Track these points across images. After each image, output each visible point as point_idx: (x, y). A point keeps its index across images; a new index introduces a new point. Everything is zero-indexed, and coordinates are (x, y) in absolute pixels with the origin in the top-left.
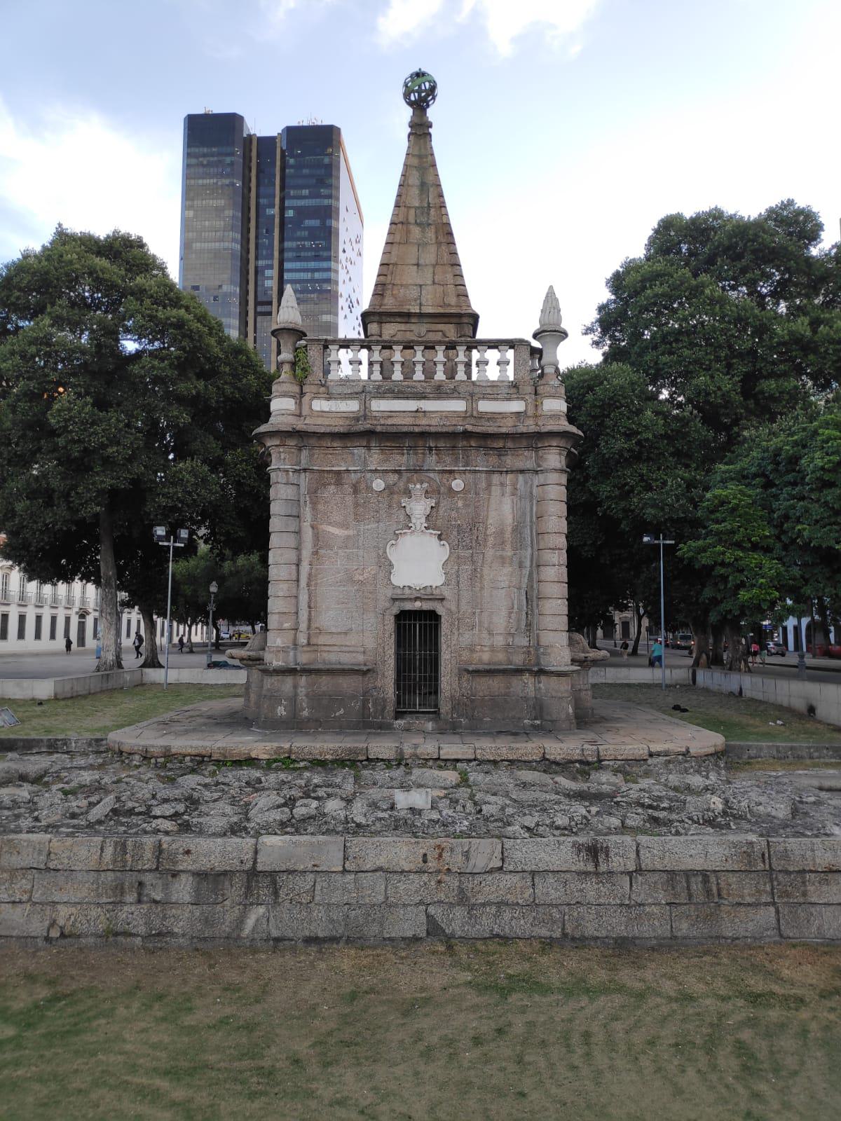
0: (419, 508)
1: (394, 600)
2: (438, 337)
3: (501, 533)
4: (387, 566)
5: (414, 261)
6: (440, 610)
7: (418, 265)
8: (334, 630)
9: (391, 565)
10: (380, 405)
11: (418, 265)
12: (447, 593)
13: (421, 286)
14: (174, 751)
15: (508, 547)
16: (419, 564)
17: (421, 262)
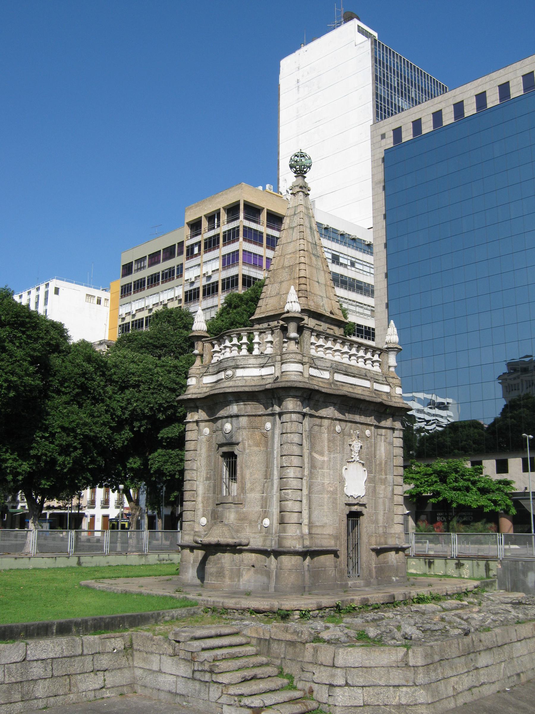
0: (357, 445)
1: (346, 504)
2: (331, 332)
3: (380, 464)
4: (342, 481)
5: (316, 280)
6: (364, 510)
7: (318, 282)
10: (339, 377)
11: (318, 282)
12: (364, 501)
13: (322, 297)
14: (323, 605)
15: (383, 473)
16: (355, 483)
17: (320, 281)
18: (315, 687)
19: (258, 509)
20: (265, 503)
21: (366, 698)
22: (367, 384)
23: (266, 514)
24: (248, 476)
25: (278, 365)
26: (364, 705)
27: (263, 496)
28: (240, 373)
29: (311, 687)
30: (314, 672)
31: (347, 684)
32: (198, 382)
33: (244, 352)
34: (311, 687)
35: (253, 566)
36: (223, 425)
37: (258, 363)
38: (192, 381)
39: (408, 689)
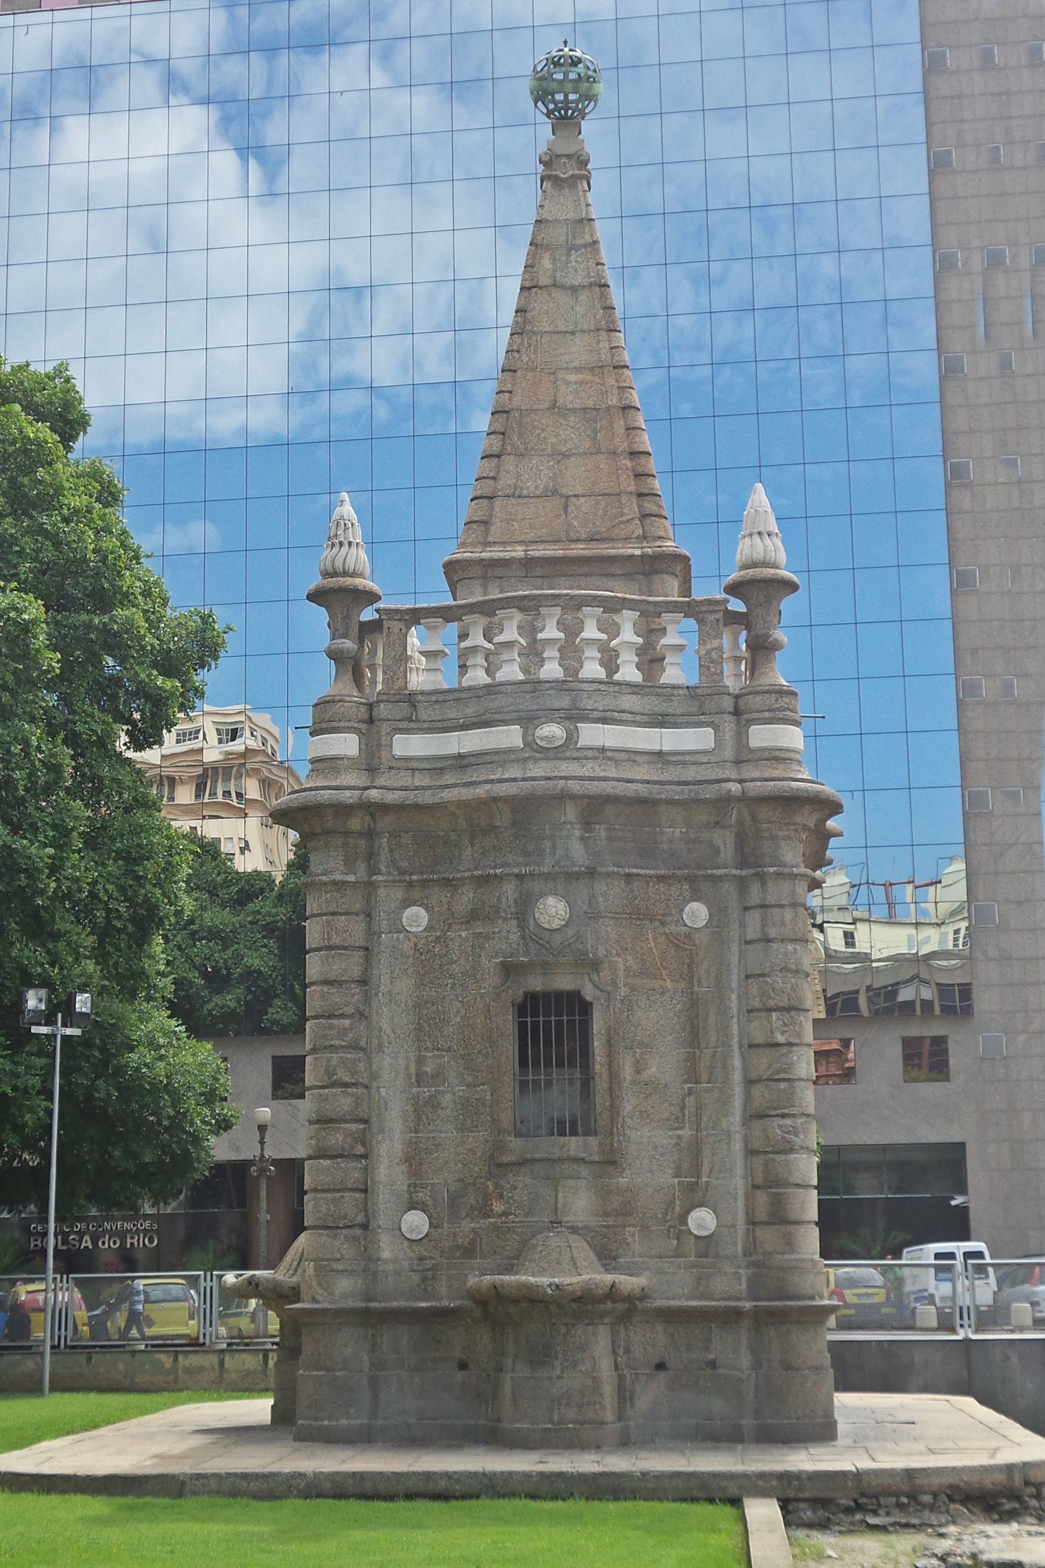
19: (667, 1179)
20: (691, 1159)
23: (694, 1195)
24: (627, 1073)
25: (729, 724)
27: (679, 1137)
28: (592, 735)
37: (647, 709)
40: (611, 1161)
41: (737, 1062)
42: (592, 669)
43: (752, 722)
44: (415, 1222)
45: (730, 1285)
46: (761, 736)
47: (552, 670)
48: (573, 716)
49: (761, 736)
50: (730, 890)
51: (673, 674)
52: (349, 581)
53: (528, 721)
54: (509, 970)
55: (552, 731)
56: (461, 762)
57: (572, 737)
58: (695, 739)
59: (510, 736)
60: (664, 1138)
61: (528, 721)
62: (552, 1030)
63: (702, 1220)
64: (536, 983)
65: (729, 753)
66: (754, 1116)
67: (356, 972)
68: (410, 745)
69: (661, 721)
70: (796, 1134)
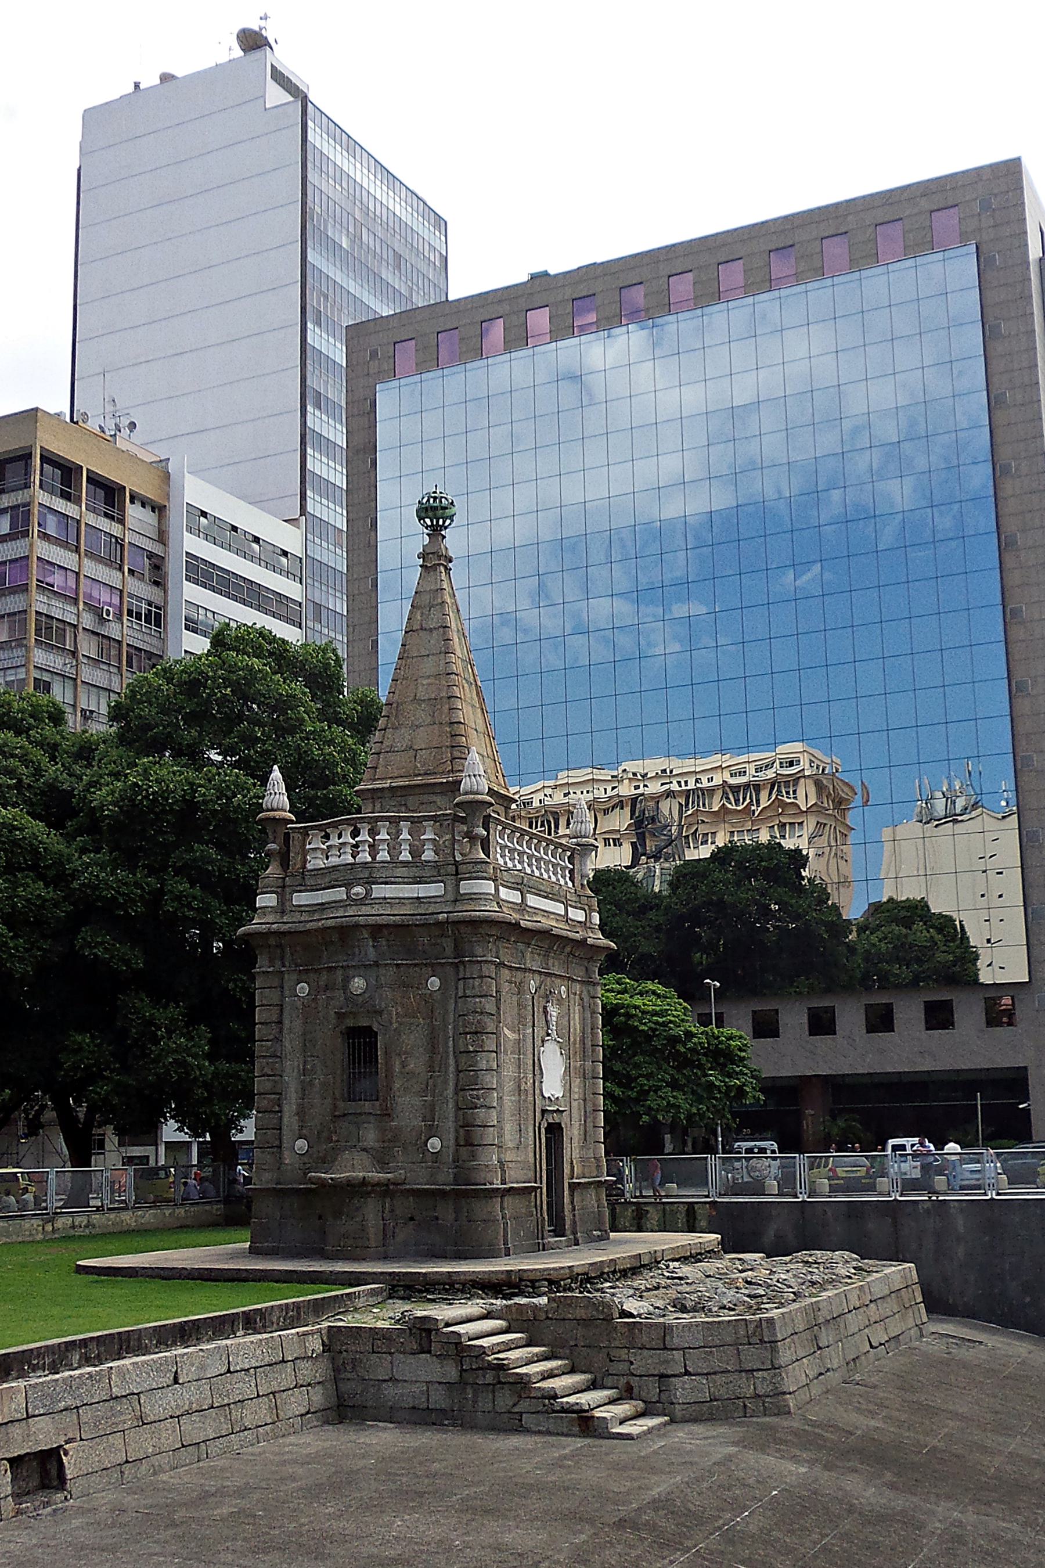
1: (544, 1112)
8: (510, 1145)
9: (542, 1073)
10: (532, 900)
18: (634, 1381)
19: (418, 1123)
20: (430, 1114)
21: (712, 1389)
22: (560, 909)
23: (432, 1131)
25: (451, 881)
26: (711, 1400)
28: (379, 891)
29: (628, 1383)
30: (632, 1359)
31: (687, 1373)
32: (283, 900)
33: (383, 855)
34: (628, 1383)
35: (412, 1219)
36: (347, 980)
38: (265, 900)
39: (765, 1374)
40: (387, 1114)
41: (451, 1061)
42: (383, 855)
43: (462, 879)
44: (301, 1145)
45: (445, 1179)
46: (465, 887)
47: (365, 856)
48: (370, 882)
49: (465, 887)
50: (450, 970)
51: (428, 855)
52: (271, 814)
53: (348, 886)
54: (340, 1016)
55: (359, 890)
56: (323, 906)
57: (369, 892)
58: (434, 889)
59: (340, 893)
60: (417, 1101)
61: (348, 886)
62: (361, 1045)
63: (434, 1144)
64: (350, 1023)
65: (450, 897)
66: (459, 1089)
67: (275, 1018)
68: (301, 899)
69: (419, 881)
70: (479, 1099)
